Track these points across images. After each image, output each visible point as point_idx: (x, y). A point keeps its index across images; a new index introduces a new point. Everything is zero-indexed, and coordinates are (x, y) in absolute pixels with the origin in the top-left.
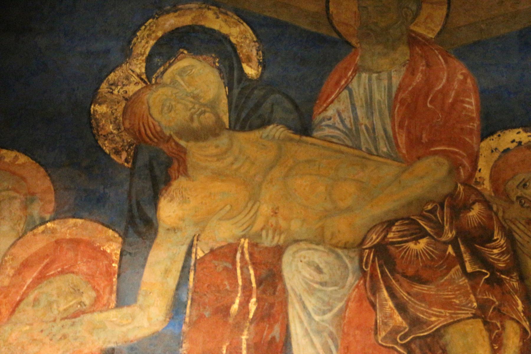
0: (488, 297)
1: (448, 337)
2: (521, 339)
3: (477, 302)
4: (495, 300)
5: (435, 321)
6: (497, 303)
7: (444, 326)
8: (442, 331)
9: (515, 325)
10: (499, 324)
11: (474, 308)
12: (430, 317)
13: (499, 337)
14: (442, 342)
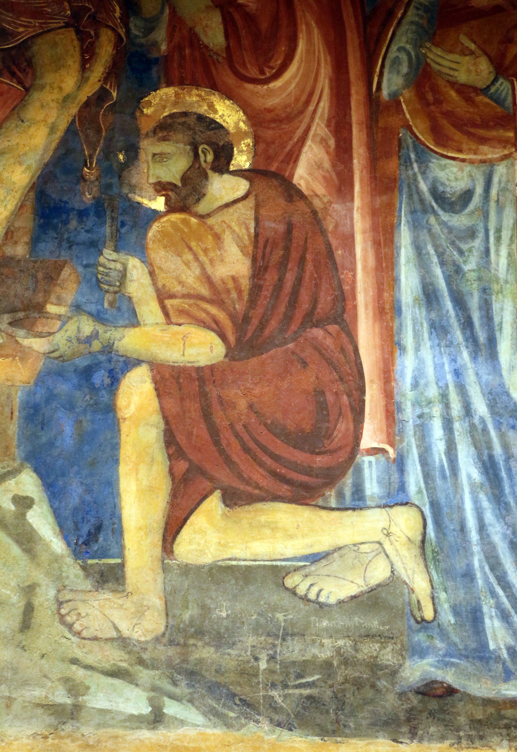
0: (83, 4)
1: (35, 48)
2: (114, 47)
3: (71, 10)
4: (91, 7)
5: (22, 32)
6: (93, 10)
7: (33, 37)
8: (29, 43)
9: (110, 33)
10: (92, 33)
11: (66, 17)
12: (17, 28)
13: (92, 46)
14: (29, 54)
